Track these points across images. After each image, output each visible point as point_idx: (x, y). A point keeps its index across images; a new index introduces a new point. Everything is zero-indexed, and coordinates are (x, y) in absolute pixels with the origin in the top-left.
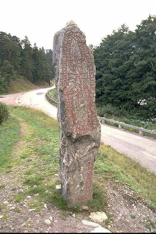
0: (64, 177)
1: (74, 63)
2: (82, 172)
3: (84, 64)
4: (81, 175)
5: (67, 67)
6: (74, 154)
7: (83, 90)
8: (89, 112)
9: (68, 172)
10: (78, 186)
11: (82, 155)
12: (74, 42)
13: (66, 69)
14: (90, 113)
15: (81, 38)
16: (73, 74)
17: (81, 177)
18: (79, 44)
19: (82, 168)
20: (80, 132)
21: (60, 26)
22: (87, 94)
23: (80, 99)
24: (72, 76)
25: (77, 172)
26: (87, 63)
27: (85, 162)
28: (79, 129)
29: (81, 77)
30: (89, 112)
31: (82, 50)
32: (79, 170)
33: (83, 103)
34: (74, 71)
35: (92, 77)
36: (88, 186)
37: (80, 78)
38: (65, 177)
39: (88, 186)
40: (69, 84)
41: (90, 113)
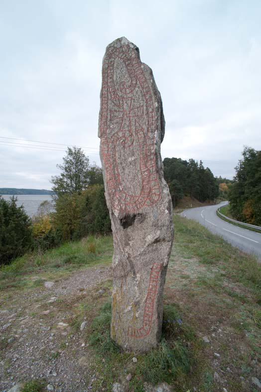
3: (137, 93)
4: (136, 288)
6: (123, 249)
7: (134, 134)
8: (144, 172)
12: (117, 61)
13: (108, 106)
14: (146, 173)
18: (127, 63)
19: (138, 275)
20: (126, 207)
22: (141, 141)
24: (117, 114)
25: (129, 279)
26: (141, 89)
27: (145, 264)
30: (144, 172)
32: (134, 278)
33: (133, 155)
34: (119, 106)
35: (150, 110)
37: (130, 117)
40: (111, 126)
41: (146, 173)
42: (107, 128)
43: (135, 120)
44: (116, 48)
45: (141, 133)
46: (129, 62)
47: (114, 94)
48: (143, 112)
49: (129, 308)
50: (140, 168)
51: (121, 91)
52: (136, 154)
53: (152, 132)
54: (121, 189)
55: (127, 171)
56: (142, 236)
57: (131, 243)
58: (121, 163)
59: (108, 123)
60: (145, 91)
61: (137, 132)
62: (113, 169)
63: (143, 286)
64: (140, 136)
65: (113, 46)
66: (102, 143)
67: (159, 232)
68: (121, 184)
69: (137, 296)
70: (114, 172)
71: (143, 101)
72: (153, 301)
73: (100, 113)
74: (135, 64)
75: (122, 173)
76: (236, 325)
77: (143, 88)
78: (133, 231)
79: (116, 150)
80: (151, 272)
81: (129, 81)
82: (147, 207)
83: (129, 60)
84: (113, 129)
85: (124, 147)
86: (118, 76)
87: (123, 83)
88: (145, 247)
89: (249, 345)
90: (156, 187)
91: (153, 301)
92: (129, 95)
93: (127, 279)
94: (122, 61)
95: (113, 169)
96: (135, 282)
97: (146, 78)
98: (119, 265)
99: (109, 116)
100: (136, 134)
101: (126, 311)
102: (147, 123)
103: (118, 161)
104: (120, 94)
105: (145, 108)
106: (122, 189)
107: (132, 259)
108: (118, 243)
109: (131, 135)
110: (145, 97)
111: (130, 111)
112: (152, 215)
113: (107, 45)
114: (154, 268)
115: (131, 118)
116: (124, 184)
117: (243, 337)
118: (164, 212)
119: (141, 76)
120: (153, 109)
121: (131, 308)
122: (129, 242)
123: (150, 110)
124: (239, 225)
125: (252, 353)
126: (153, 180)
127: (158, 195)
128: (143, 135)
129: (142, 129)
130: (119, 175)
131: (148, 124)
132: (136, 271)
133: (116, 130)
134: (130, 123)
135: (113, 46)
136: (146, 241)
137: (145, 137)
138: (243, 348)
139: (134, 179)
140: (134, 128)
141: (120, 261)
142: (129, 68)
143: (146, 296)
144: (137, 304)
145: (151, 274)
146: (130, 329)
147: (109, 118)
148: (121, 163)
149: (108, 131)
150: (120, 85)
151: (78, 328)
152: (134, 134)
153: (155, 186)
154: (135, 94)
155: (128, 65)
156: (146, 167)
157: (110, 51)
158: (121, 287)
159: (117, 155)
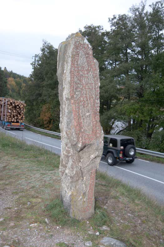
0: (66, 189)
1: (81, 73)
3: (90, 75)
4: (84, 185)
5: (75, 77)
7: (88, 99)
8: (94, 121)
9: (72, 182)
10: (81, 197)
11: (85, 164)
13: (74, 79)
14: (95, 122)
15: (88, 50)
16: (80, 84)
18: (87, 56)
19: (85, 178)
21: (41, 46)
22: (92, 104)
24: (79, 85)
25: (80, 181)
26: (93, 73)
28: (84, 137)
29: (87, 87)
30: (94, 121)
32: (82, 180)
34: (80, 81)
37: (86, 88)
38: (68, 189)
40: (77, 93)
42: (74, 94)
44: (81, 44)
45: (92, 99)
47: (78, 73)
49: (81, 197)
53: (97, 99)
55: (85, 121)
56: (88, 156)
57: (82, 160)
58: (83, 116)
59: (75, 90)
60: (94, 75)
63: (87, 183)
64: (92, 101)
65: (79, 42)
67: (97, 153)
68: (82, 128)
69: (84, 189)
70: (79, 121)
72: (92, 190)
76: (115, 197)
78: (82, 154)
82: (94, 140)
83: (88, 54)
84: (77, 95)
85: (84, 106)
87: (83, 67)
88: (90, 161)
89: (122, 203)
90: (99, 130)
91: (92, 190)
92: (86, 75)
94: (84, 53)
98: (75, 174)
99: (75, 86)
100: (90, 100)
101: (79, 199)
102: (95, 94)
103: (81, 115)
104: (81, 73)
105: (94, 85)
107: (82, 169)
108: (75, 161)
109: (87, 100)
112: (96, 144)
114: (93, 172)
115: (87, 89)
117: (119, 201)
118: (101, 142)
120: (98, 87)
122: (81, 160)
123: (97, 87)
124: (40, 133)
125: (125, 206)
126: (98, 126)
129: (93, 97)
130: (81, 123)
134: (86, 92)
135: (79, 42)
136: (90, 158)
137: (94, 102)
138: (121, 206)
140: (88, 96)
141: (76, 171)
144: (84, 194)
146: (82, 209)
147: (75, 87)
149: (75, 96)
151: (46, 223)
152: (88, 99)
156: (95, 119)
157: (77, 44)
159: (80, 111)
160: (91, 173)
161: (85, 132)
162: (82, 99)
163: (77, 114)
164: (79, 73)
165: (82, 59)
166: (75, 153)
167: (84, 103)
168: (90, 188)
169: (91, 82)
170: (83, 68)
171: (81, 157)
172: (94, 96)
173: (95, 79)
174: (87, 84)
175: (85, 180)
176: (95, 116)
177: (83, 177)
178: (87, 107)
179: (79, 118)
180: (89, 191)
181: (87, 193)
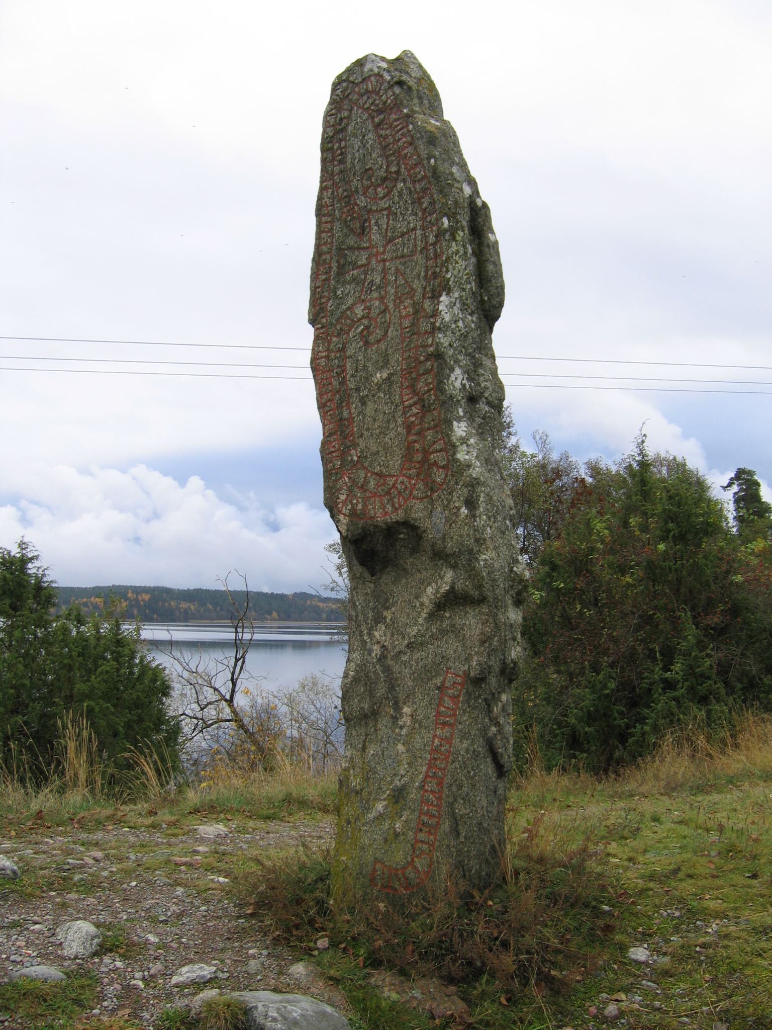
1: (362, 201)
2: (404, 732)
3: (400, 195)
4: (400, 747)
7: (391, 306)
8: (410, 406)
10: (380, 807)
14: (414, 410)
17: (399, 763)
18: (377, 120)
19: (406, 710)
22: (406, 323)
23: (372, 352)
25: (383, 723)
29: (387, 256)
31: (386, 137)
32: (395, 719)
33: (386, 363)
36: (425, 818)
39: (425, 818)
41: (414, 410)
43: (397, 269)
45: (408, 302)
46: (382, 116)
48: (415, 245)
49: (380, 807)
50: (401, 396)
51: (364, 194)
52: (392, 362)
54: (355, 458)
57: (388, 615)
58: (358, 390)
61: (398, 300)
62: (339, 406)
66: (317, 338)
71: (416, 214)
72: (440, 784)
73: (313, 259)
74: (396, 120)
75: (359, 414)
77: (414, 182)
79: (348, 354)
80: (441, 699)
81: (381, 167)
83: (380, 112)
86: (356, 155)
93: (379, 726)
95: (339, 406)
96: (397, 730)
97: (419, 156)
100: (397, 307)
102: (423, 274)
104: (362, 201)
106: (359, 457)
107: (390, 662)
108: (357, 616)
110: (421, 204)
111: (385, 247)
113: (332, 78)
116: (362, 444)
119: (409, 150)
121: (386, 807)
122: (385, 613)
127: (443, 467)
128: (411, 310)
130: (351, 419)
131: (426, 276)
132: (402, 697)
133: (350, 301)
136: (422, 604)
139: (388, 428)
142: (382, 132)
143: (424, 768)
144: (398, 795)
145: (439, 705)
148: (358, 390)
150: (362, 179)
152: (391, 306)
153: (435, 443)
154: (396, 199)
155: (379, 125)
156: (415, 393)
158: (364, 749)
159: (349, 364)
160: (439, 688)
161: (366, 464)
162: (359, 311)
163: (335, 383)
164: (356, 204)
165: (357, 144)
166: (358, 575)
167: (367, 328)
168: (430, 767)
169: (409, 223)
170: (369, 179)
171: (387, 600)
172: (417, 285)
173: (424, 205)
174: (390, 241)
175: (406, 720)
176: (416, 380)
177: (396, 703)
178: (379, 341)
179: (341, 400)
180: (422, 787)
181: (413, 795)
